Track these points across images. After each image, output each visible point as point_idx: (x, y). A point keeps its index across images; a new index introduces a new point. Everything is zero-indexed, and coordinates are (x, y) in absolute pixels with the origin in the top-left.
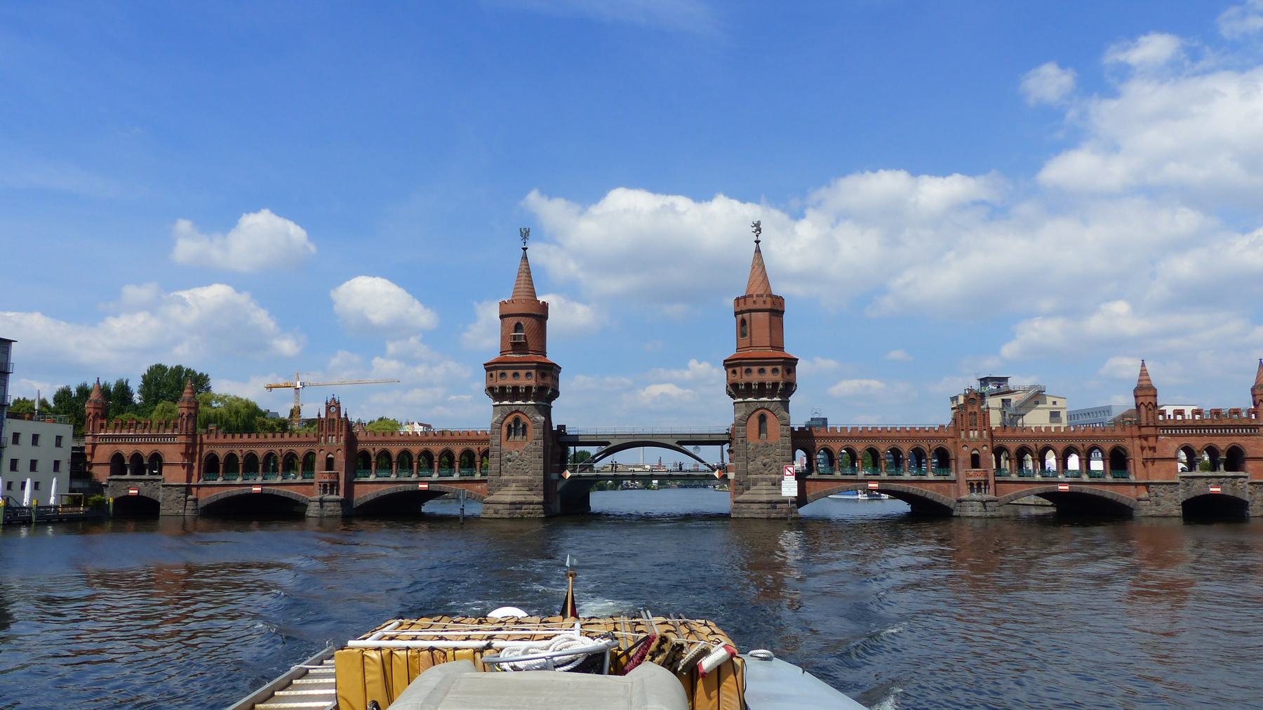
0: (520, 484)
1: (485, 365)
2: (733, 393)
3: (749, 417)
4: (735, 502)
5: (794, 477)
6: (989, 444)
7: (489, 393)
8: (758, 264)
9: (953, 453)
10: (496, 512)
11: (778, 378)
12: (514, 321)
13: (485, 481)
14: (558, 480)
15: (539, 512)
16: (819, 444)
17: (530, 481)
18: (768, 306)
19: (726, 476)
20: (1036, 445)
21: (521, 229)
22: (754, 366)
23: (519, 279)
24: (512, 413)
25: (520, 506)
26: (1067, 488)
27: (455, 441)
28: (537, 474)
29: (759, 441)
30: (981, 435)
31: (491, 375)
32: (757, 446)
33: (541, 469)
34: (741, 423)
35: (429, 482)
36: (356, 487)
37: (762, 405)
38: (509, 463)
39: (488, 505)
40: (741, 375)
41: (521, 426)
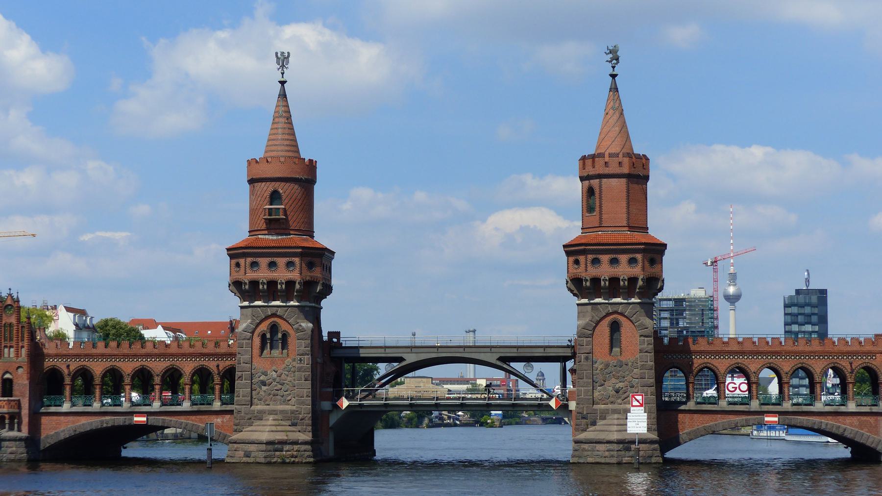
0: (279, 417)
1: (228, 250)
4: (576, 442)
5: (643, 408)
7: (232, 287)
8: (612, 108)
10: (247, 455)
11: (637, 271)
12: (269, 187)
13: (231, 412)
14: (330, 411)
15: (306, 454)
17: (292, 412)
18: (625, 170)
19: (566, 406)
21: (277, 53)
22: (602, 254)
23: (275, 126)
25: (280, 446)
28: (303, 403)
31: (238, 265)
32: (607, 366)
34: (587, 332)
35: (149, 414)
36: (44, 420)
37: (615, 308)
38: (264, 388)
39: (236, 446)
40: (586, 267)
41: (280, 335)
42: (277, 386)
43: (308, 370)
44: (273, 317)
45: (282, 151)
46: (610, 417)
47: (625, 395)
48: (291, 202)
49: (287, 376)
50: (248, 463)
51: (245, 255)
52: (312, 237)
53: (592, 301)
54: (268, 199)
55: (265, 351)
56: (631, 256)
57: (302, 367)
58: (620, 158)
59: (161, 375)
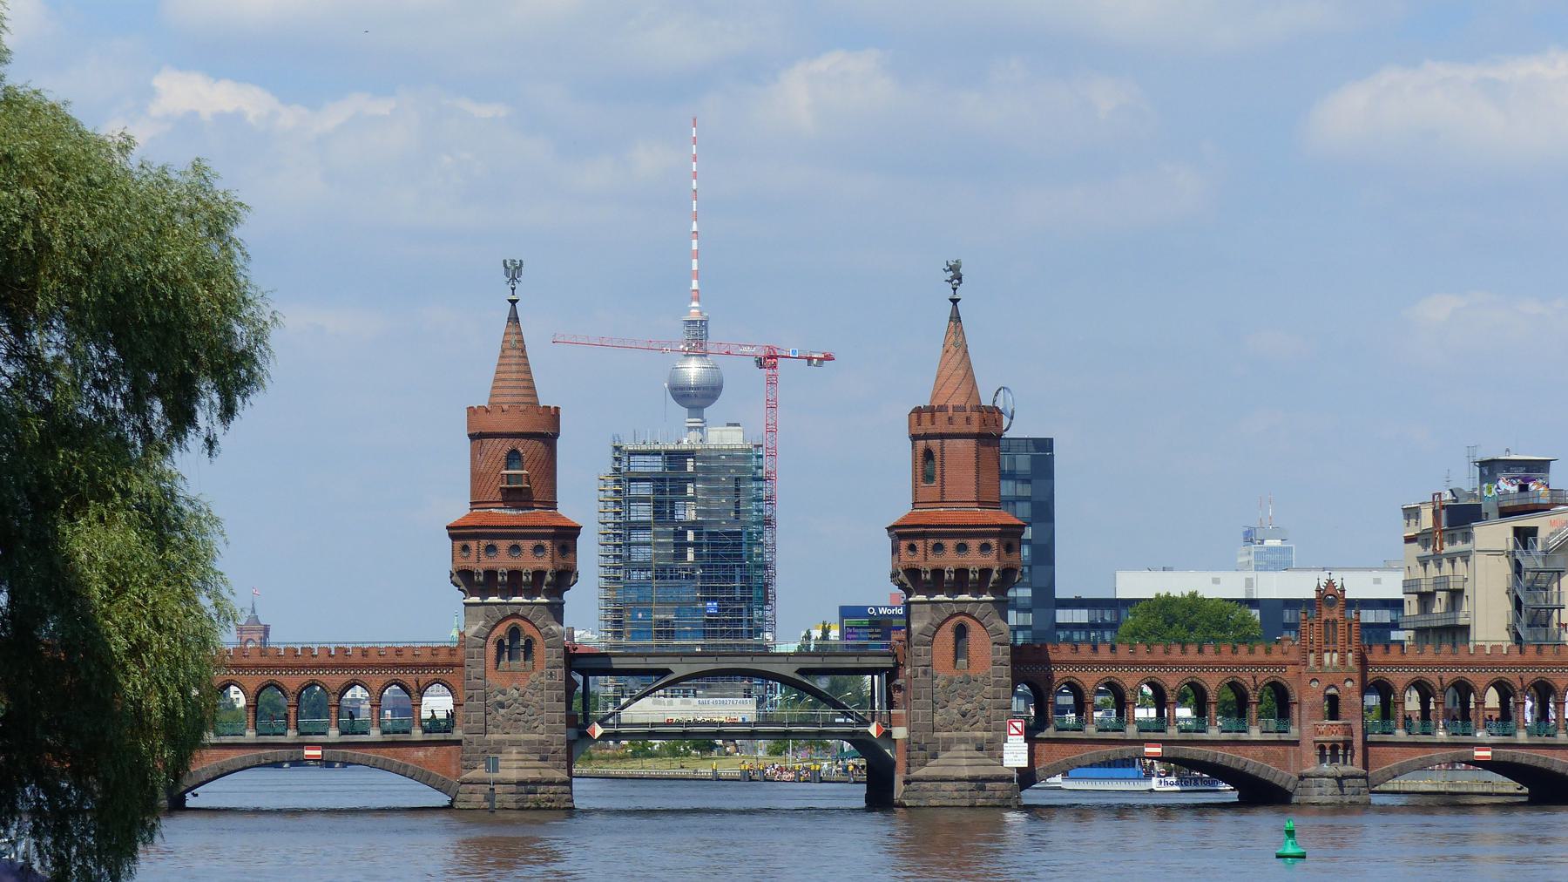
2: (909, 585)
3: (938, 628)
6: (1356, 677)
9: (1296, 692)
11: (991, 560)
12: (506, 445)
16: (1059, 674)
17: (541, 743)
18: (975, 429)
20: (1441, 679)
24: (505, 618)
26: (1489, 753)
27: (370, 666)
28: (554, 731)
29: (954, 672)
32: (951, 682)
33: (561, 722)
37: (961, 608)
38: (502, 711)
41: (522, 642)
43: (561, 688)
44: (513, 618)
46: (955, 748)
48: (533, 466)
49: (533, 695)
51: (477, 537)
53: (931, 599)
54: (503, 461)
55: (501, 663)
56: (983, 541)
58: (968, 413)
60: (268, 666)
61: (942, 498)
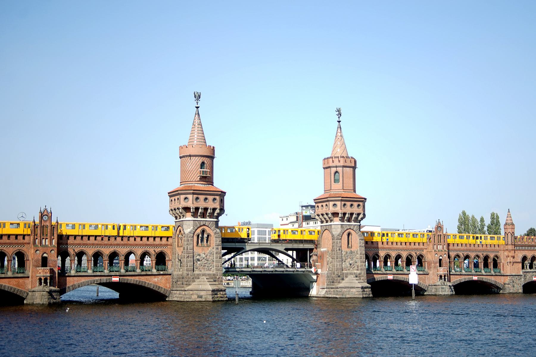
3: (343, 233)
17: (214, 275)
21: (194, 94)
24: (201, 226)
30: (443, 248)
32: (347, 253)
38: (199, 262)
42: (204, 261)
45: (202, 142)
47: (353, 266)
50: (200, 301)
52: (213, 185)
54: (200, 166)
57: (218, 252)
59: (125, 255)
60: (97, 244)
61: (331, 188)
